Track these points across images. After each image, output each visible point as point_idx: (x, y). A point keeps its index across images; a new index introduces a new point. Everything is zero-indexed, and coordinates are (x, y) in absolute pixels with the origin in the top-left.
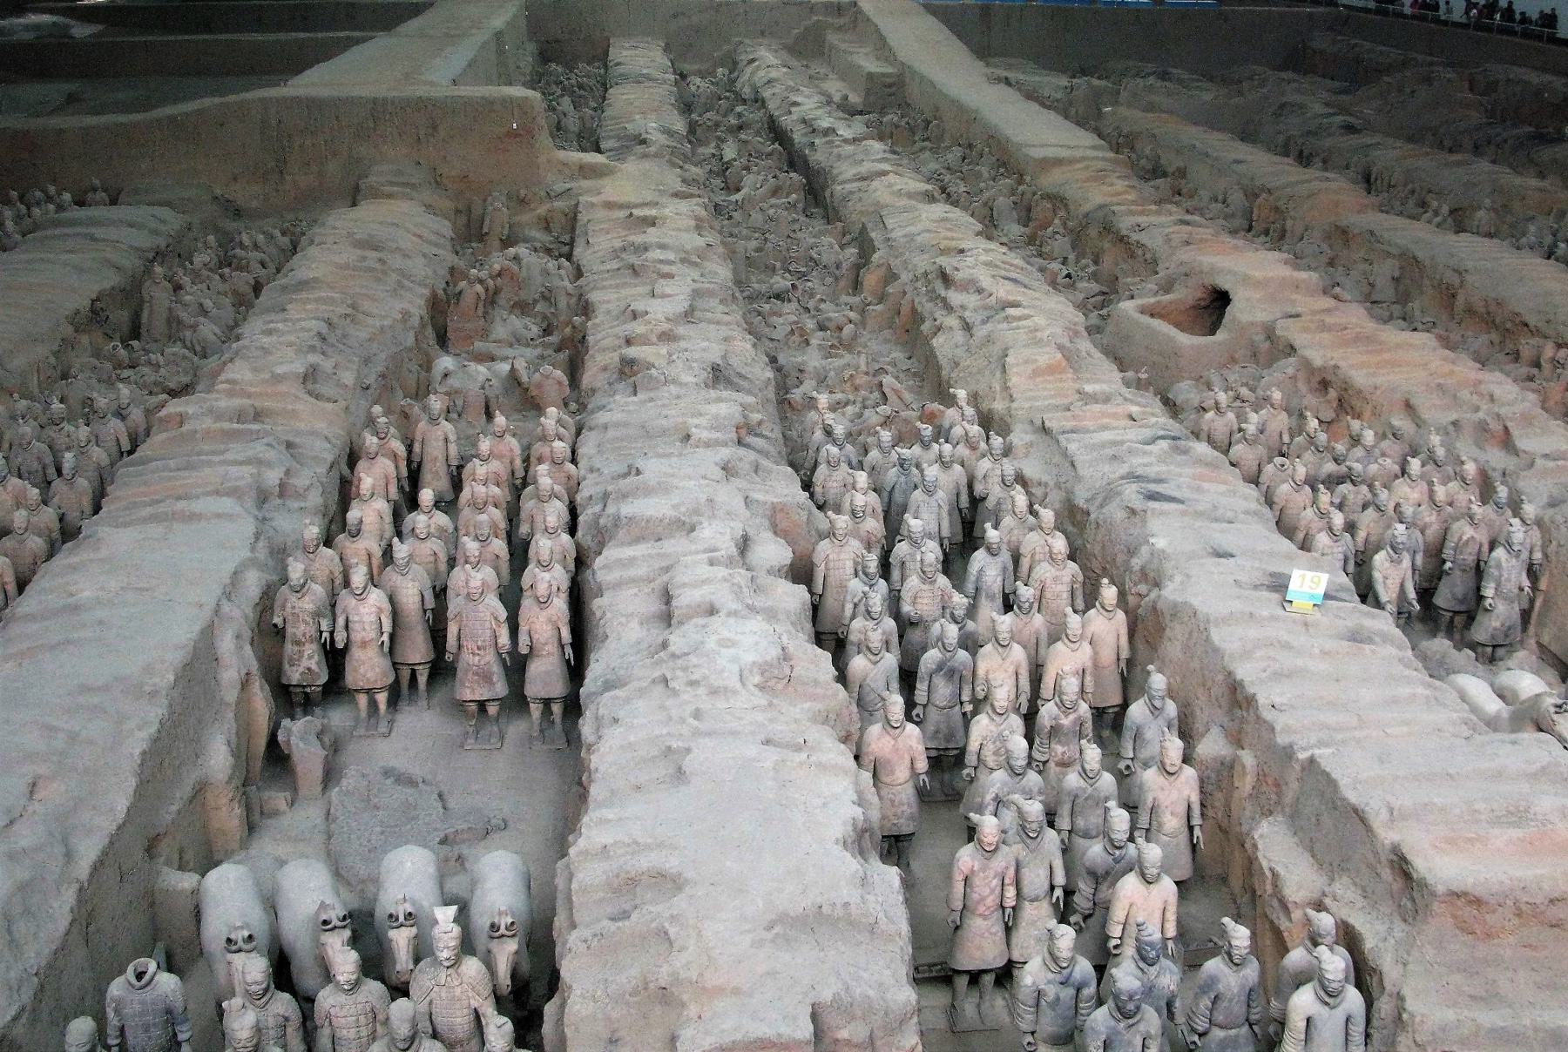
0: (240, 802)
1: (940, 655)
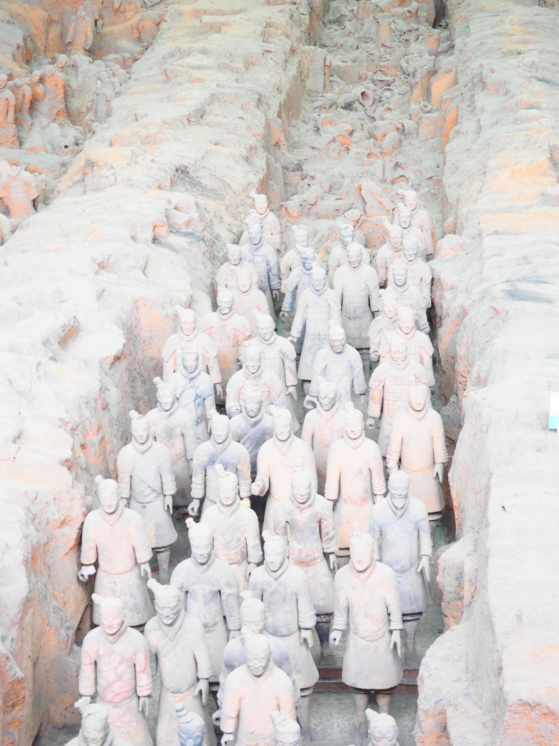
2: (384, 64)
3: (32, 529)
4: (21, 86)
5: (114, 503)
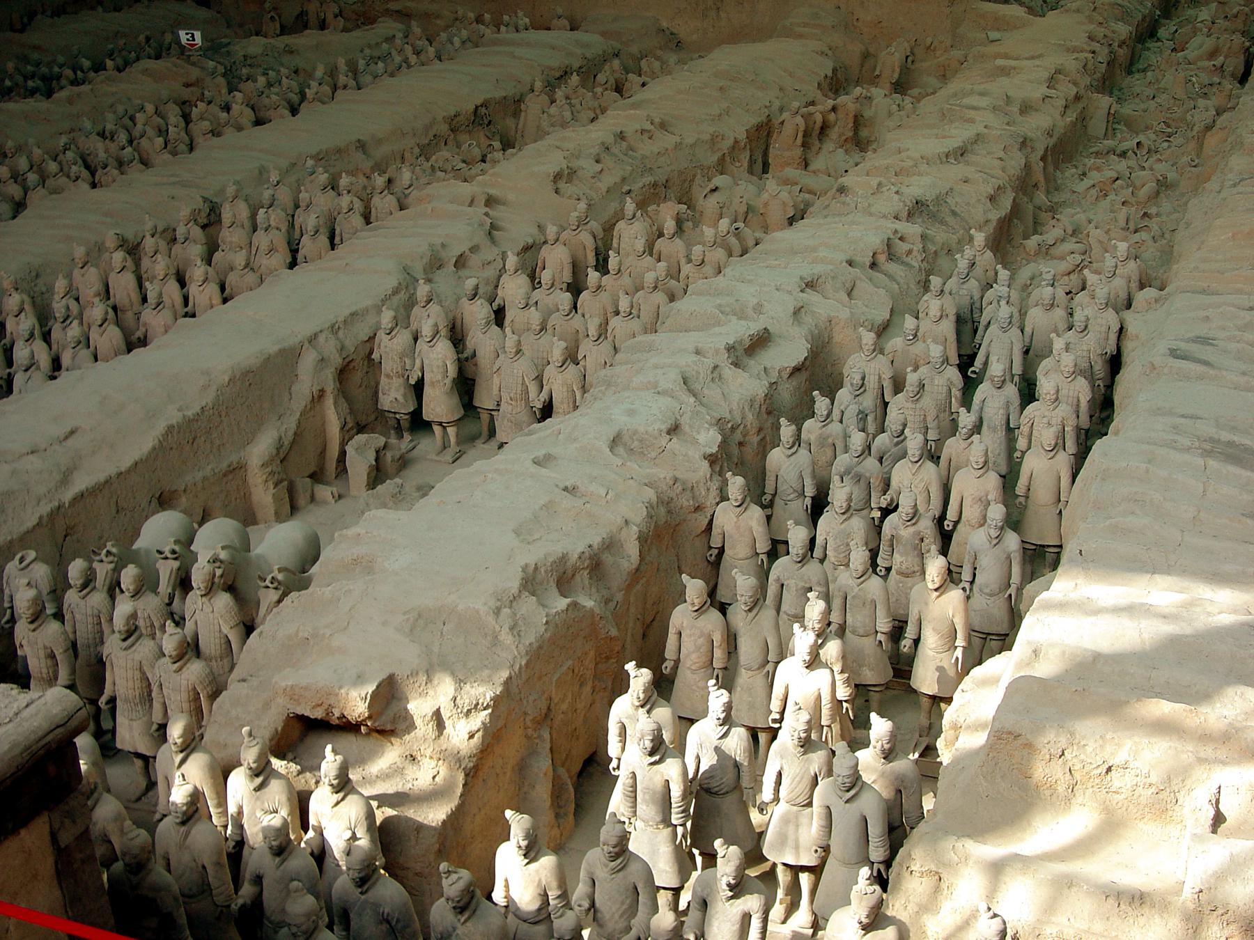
0: (276, 485)
1: (848, 460)
2: (1168, 115)
3: (662, 510)
4: (813, 114)
5: (740, 498)
